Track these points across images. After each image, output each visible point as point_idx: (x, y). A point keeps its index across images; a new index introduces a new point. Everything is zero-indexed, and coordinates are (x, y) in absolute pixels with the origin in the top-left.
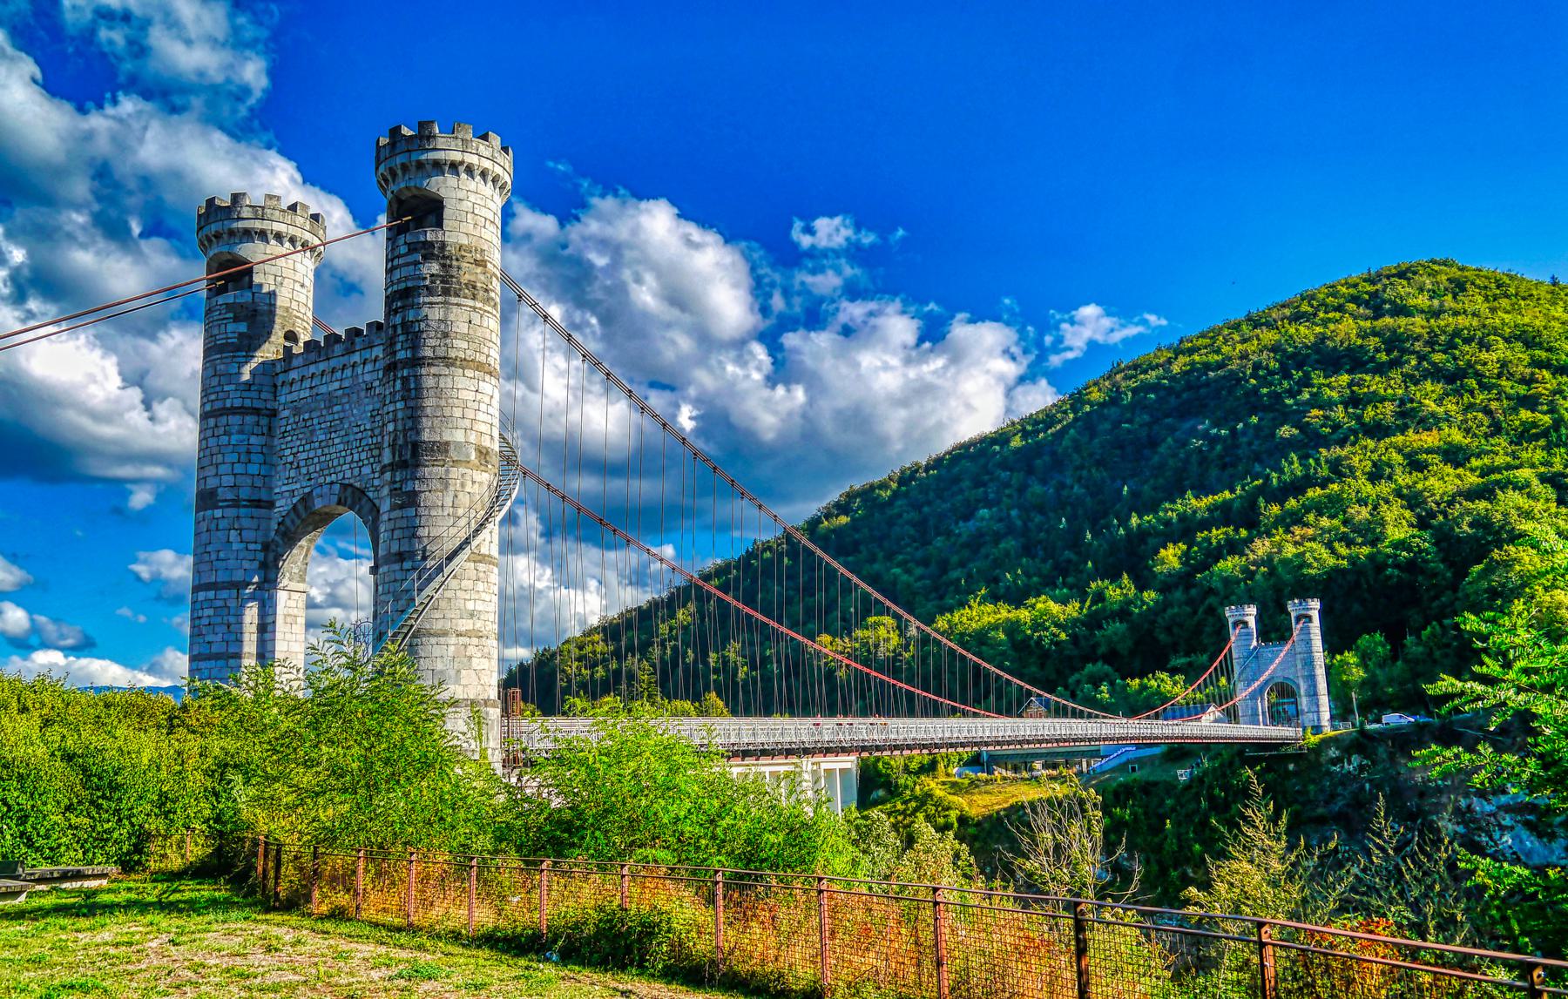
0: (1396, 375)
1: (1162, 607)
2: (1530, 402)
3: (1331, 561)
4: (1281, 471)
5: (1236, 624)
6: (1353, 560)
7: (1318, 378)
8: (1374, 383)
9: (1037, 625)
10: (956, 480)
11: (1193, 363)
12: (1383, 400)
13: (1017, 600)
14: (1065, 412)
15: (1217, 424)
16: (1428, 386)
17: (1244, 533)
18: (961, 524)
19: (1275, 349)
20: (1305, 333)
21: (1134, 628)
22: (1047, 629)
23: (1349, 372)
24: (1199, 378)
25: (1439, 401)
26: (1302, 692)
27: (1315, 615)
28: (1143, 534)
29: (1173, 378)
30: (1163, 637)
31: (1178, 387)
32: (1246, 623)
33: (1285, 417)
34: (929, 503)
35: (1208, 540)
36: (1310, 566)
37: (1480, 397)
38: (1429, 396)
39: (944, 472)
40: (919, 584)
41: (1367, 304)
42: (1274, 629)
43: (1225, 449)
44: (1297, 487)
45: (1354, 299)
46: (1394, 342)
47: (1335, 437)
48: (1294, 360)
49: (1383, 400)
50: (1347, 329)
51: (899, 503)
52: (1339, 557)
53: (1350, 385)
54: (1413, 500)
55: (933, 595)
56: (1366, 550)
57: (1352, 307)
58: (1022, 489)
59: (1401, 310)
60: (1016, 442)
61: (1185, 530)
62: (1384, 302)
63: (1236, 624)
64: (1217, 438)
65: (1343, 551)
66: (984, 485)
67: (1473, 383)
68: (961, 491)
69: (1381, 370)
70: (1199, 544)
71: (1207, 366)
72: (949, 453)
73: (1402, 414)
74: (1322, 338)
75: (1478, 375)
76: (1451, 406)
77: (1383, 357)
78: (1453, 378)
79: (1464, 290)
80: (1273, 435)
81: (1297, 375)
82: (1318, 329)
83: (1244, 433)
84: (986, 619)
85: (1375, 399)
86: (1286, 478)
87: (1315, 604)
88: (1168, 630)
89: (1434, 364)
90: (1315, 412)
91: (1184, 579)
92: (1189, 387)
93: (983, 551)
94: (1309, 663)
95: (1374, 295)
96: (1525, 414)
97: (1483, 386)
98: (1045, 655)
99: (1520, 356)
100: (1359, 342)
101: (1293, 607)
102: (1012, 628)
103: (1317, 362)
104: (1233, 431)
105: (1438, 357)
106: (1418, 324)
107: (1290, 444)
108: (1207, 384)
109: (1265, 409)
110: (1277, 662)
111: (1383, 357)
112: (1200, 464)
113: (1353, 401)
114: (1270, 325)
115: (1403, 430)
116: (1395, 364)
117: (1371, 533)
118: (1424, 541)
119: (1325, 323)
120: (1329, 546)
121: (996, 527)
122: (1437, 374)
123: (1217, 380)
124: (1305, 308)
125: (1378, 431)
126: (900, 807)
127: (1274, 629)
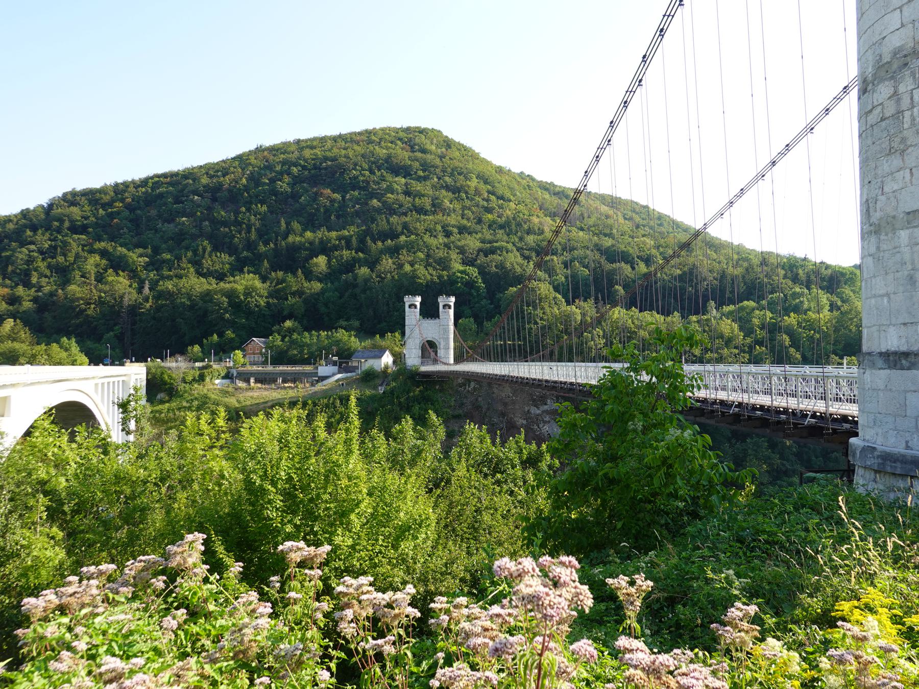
0: (428, 183)
1: (323, 291)
2: (489, 210)
3: (429, 277)
4: (377, 225)
5: (410, 306)
6: (440, 277)
7: (389, 177)
8: (417, 186)
9: (248, 294)
10: (161, 195)
11: (316, 155)
12: (423, 196)
13: (221, 277)
14: (235, 167)
15: (334, 191)
16: (444, 192)
17: (361, 255)
18: (166, 225)
19: (363, 156)
20: (382, 152)
21: (306, 301)
22: (252, 297)
23: (405, 177)
24: (321, 164)
25: (451, 202)
26: (442, 347)
27: (452, 304)
28: (294, 249)
29: (306, 160)
30: (323, 309)
31: (309, 167)
32: (415, 307)
33: (373, 195)
34: (140, 208)
35: (342, 256)
36: (419, 278)
37: (468, 203)
38: (446, 198)
39: (150, 190)
40: (140, 259)
41: (406, 143)
42: (430, 311)
43: (340, 207)
44: (394, 235)
45: (400, 139)
46: (425, 166)
47: (400, 210)
48: (376, 165)
49: (423, 196)
50: (402, 155)
51: (117, 204)
52: (431, 275)
53: (406, 184)
54: (462, 251)
55: (150, 268)
56: (445, 273)
57: (399, 142)
58: (209, 209)
59: (424, 151)
60: (205, 180)
61: (324, 248)
62: (415, 145)
63: (410, 306)
64: (333, 201)
65: (431, 270)
66: (183, 203)
67: (464, 195)
68: (165, 204)
69: (419, 179)
70: (335, 258)
71: (326, 159)
72: (152, 178)
73: (433, 205)
74: (389, 157)
75: (466, 193)
76: (458, 206)
77: (421, 173)
78: (456, 190)
79: (450, 148)
80: (367, 204)
81: (378, 173)
82: (384, 151)
83: (350, 200)
84: (206, 287)
85: (421, 195)
86: (379, 228)
87: (453, 299)
88: (326, 305)
89: (446, 182)
90: (389, 195)
91: (331, 276)
92: (315, 167)
93: (184, 244)
94: (446, 331)
95: (410, 140)
96: (490, 216)
97: (467, 198)
98: (249, 313)
99: (483, 188)
100: (409, 163)
101: (442, 300)
102: (231, 295)
103: (387, 168)
104: (343, 197)
105: (447, 179)
106: (437, 162)
107: (378, 211)
108: (326, 169)
109: (360, 188)
110: (429, 329)
111: (421, 173)
112: (325, 212)
113: (407, 193)
114: (358, 143)
115: (434, 213)
116: (425, 178)
117: (444, 264)
118: (473, 271)
119: (387, 148)
120: (425, 267)
121: (194, 231)
122: (447, 188)
123: (330, 167)
124: (373, 138)
125: (421, 211)
126: (185, 404)
127: (430, 311)
